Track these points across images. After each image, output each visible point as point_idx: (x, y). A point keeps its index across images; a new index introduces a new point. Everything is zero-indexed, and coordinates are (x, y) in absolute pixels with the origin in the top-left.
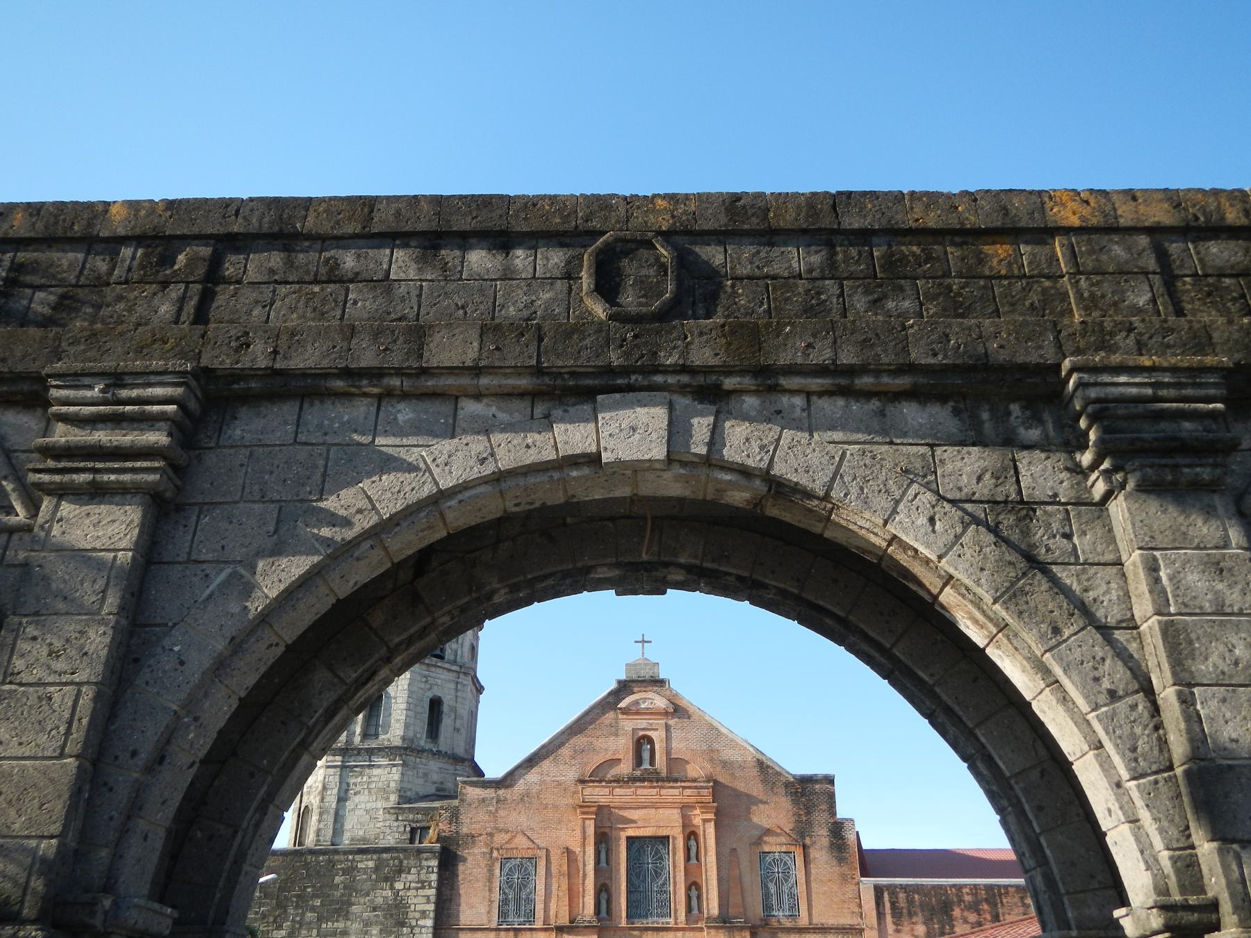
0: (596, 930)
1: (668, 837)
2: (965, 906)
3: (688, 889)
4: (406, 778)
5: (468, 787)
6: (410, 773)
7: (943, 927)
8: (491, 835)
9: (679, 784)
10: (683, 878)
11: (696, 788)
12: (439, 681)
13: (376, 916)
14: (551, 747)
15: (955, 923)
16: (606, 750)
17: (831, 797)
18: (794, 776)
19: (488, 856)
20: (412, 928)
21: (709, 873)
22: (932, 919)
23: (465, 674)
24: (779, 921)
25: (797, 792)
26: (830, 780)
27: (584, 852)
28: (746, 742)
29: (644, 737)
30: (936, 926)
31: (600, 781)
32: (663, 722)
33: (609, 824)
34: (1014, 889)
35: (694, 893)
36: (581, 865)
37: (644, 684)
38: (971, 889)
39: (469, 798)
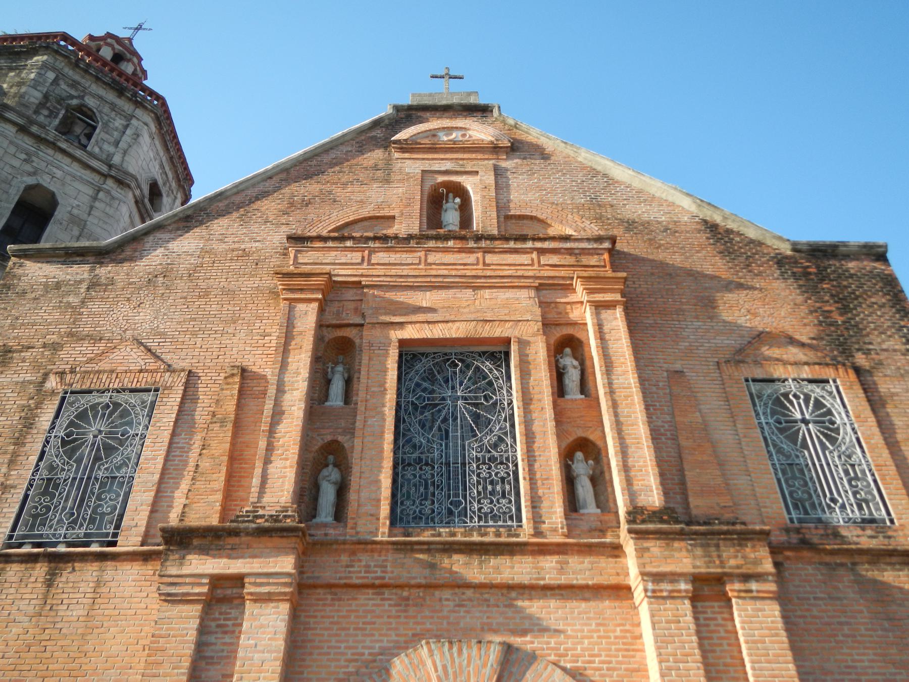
0: (292, 542)
1: (508, 341)
3: (567, 457)
5: (28, 263)
8: (55, 347)
9: (529, 244)
10: (551, 425)
11: (570, 252)
12: (55, 170)
14: (238, 199)
16: (361, 201)
17: (891, 283)
18: (796, 247)
19: (31, 389)
21: (623, 410)
23: (120, 182)
25: (806, 274)
26: (878, 254)
27: (284, 365)
29: (446, 184)
31: (342, 239)
32: (492, 162)
33: (358, 320)
35: (582, 467)
36: (272, 391)
37: (446, 114)
39: (23, 284)
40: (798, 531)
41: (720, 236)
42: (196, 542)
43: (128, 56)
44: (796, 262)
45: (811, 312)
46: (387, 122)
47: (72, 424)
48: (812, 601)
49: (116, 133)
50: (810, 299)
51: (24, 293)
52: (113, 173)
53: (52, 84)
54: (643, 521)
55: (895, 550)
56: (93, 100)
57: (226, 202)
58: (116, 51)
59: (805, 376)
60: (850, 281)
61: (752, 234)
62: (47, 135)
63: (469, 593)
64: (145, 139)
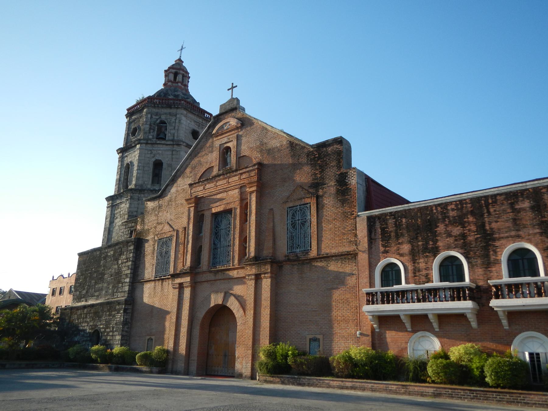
2: (450, 221)
4: (133, 206)
6: (136, 202)
7: (427, 243)
8: (155, 227)
11: (248, 172)
12: (159, 151)
13: (112, 279)
15: (439, 238)
16: (207, 163)
20: (122, 283)
21: (251, 228)
22: (417, 238)
23: (178, 145)
24: (297, 256)
28: (282, 131)
30: (420, 243)
34: (503, 197)
38: (456, 205)
40: (288, 256)
41: (293, 148)
42: (176, 276)
43: (178, 71)
44: (313, 153)
45: (312, 175)
46: (212, 124)
47: (160, 248)
48: (287, 275)
49: (173, 124)
50: (313, 169)
51: (148, 213)
52: (174, 143)
53: (150, 119)
54: (247, 262)
55: (307, 259)
56: (163, 116)
57: (180, 171)
58: (174, 72)
59: (302, 203)
60: (327, 157)
61: (302, 144)
62: (153, 141)
63: (222, 281)
64: (184, 118)
